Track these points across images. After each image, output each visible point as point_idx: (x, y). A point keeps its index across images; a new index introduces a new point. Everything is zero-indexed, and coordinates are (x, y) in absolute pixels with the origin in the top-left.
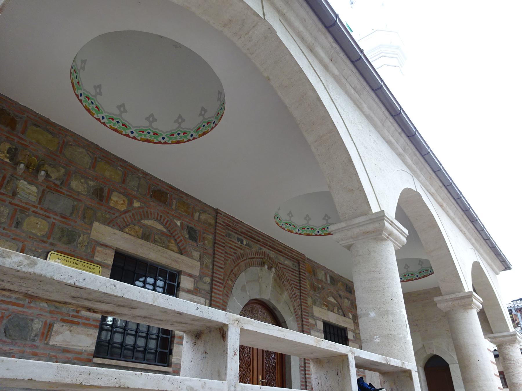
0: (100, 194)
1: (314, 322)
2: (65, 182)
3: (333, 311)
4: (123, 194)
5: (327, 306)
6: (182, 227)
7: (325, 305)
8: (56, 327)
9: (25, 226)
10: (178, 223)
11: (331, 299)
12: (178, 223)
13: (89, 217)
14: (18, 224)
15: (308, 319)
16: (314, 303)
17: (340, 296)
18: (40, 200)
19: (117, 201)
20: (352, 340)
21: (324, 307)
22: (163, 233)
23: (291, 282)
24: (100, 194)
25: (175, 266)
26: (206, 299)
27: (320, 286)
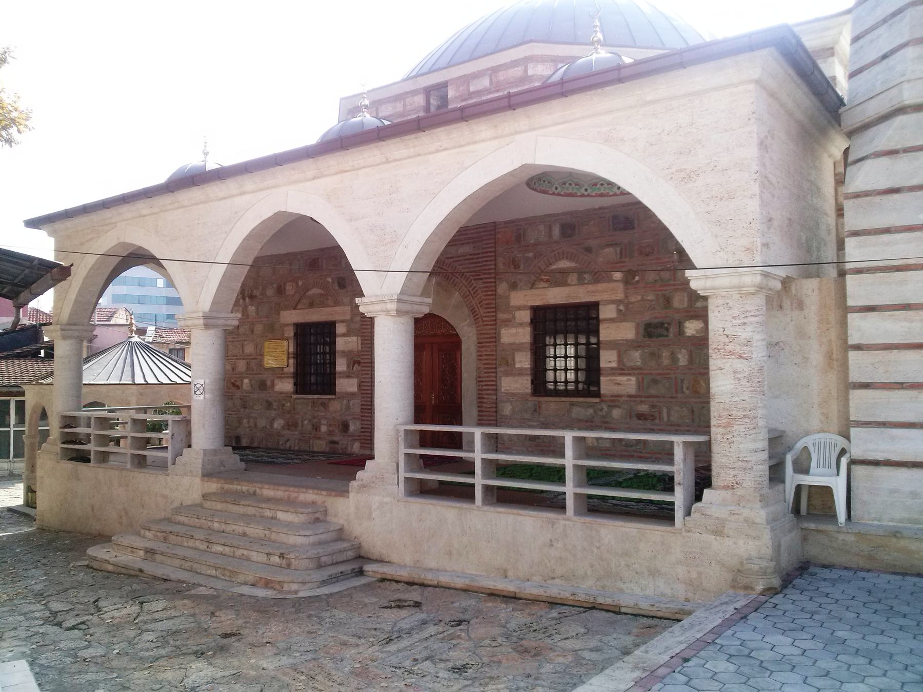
0: (280, 291)
1: (510, 316)
2: (263, 294)
3: (565, 284)
4: (291, 281)
5: (547, 281)
6: (333, 282)
7: (542, 280)
8: (276, 381)
9: (255, 332)
10: (330, 280)
11: (564, 264)
12: (330, 280)
13: (278, 309)
14: (253, 331)
15: (495, 316)
16: (514, 286)
17: (588, 250)
18: (257, 313)
19: (290, 289)
20: (612, 320)
21: (543, 284)
22: (321, 295)
23: (468, 275)
24: (280, 291)
25: (330, 318)
26: (358, 336)
27: (531, 255)
